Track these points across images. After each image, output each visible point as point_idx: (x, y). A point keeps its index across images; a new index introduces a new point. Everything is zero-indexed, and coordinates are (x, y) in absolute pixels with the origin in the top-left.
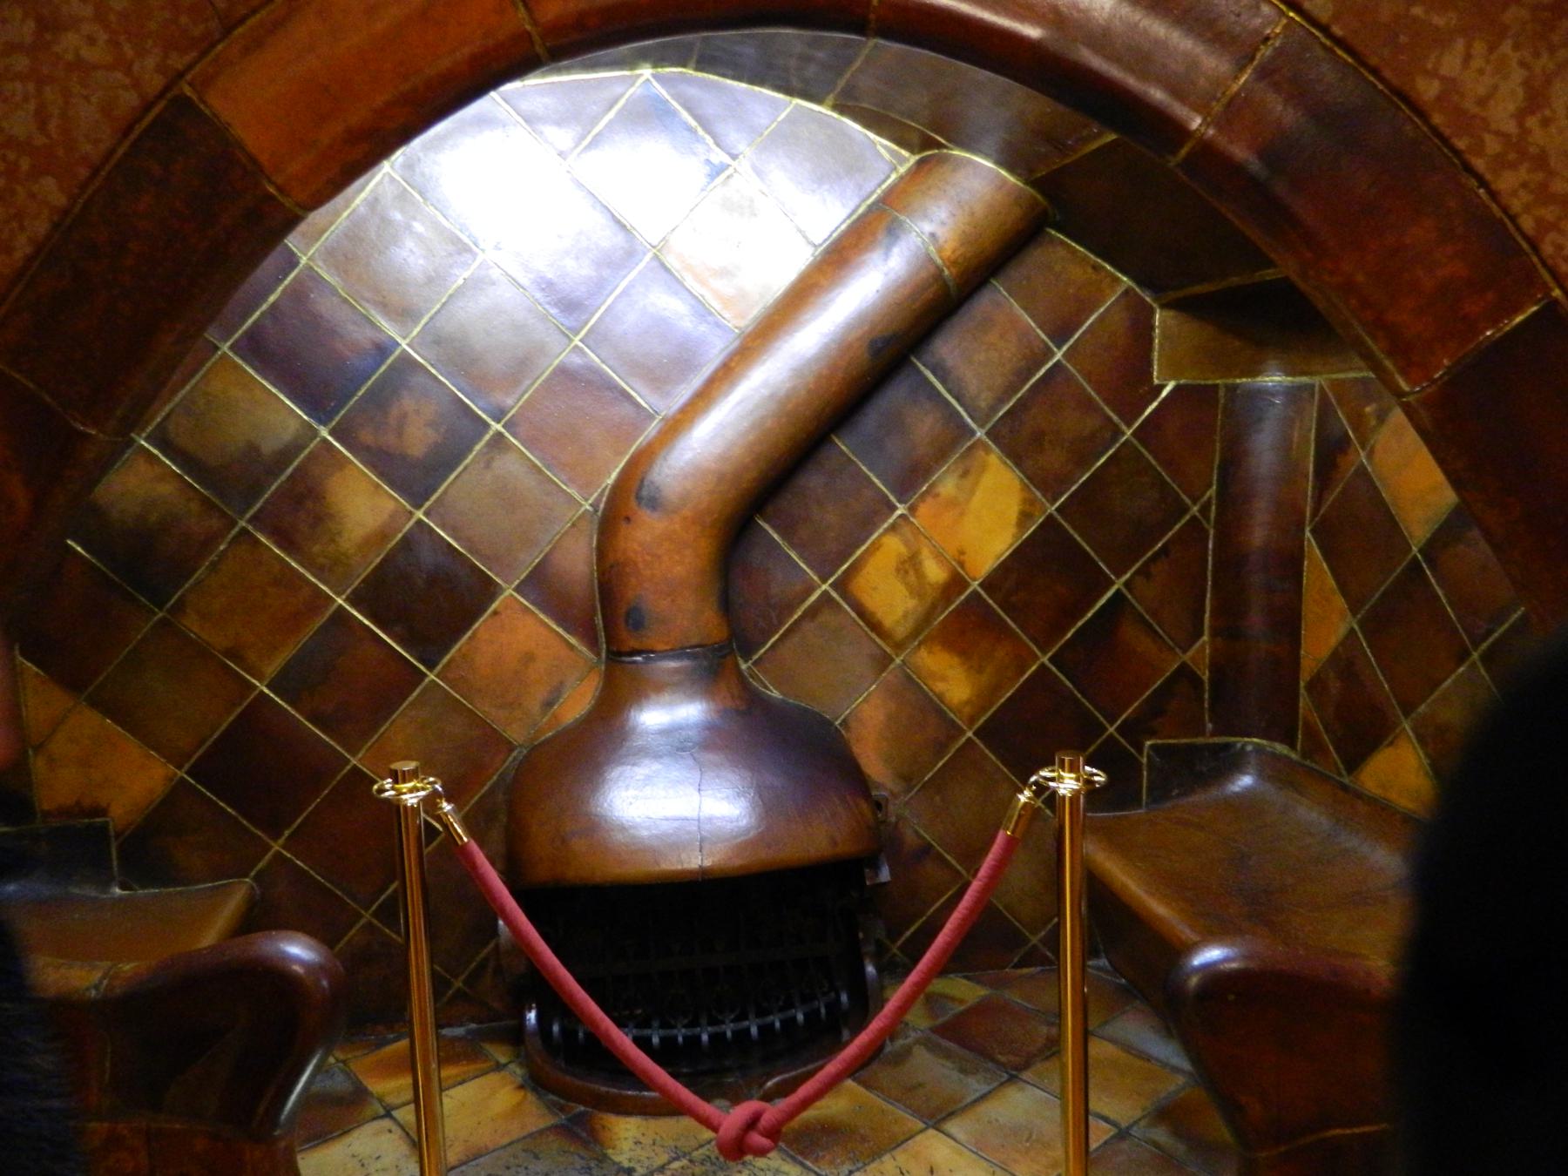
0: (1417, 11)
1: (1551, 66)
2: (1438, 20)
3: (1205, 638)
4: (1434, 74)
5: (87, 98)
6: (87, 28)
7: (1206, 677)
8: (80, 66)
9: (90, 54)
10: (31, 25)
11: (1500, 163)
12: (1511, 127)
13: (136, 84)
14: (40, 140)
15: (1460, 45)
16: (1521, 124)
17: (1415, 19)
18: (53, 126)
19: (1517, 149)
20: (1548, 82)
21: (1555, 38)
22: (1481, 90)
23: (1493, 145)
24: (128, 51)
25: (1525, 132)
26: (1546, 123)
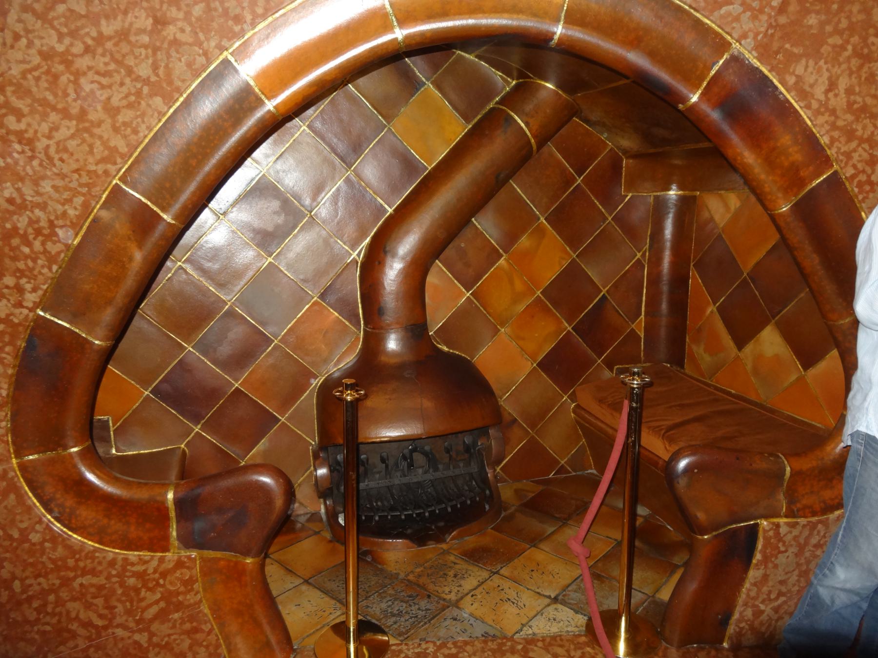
0: (787, 46)
1: (839, 72)
2: (796, 50)
3: (643, 316)
4: (793, 73)
5: (180, 61)
6: (180, 24)
7: (642, 336)
8: (175, 43)
10: (150, 21)
11: (817, 113)
13: (205, 54)
15: (804, 61)
16: (826, 96)
17: (787, 49)
18: (161, 72)
19: (825, 108)
20: (838, 78)
21: (841, 59)
22: (812, 81)
23: (815, 105)
24: (201, 36)
25: (828, 99)
26: (836, 95)
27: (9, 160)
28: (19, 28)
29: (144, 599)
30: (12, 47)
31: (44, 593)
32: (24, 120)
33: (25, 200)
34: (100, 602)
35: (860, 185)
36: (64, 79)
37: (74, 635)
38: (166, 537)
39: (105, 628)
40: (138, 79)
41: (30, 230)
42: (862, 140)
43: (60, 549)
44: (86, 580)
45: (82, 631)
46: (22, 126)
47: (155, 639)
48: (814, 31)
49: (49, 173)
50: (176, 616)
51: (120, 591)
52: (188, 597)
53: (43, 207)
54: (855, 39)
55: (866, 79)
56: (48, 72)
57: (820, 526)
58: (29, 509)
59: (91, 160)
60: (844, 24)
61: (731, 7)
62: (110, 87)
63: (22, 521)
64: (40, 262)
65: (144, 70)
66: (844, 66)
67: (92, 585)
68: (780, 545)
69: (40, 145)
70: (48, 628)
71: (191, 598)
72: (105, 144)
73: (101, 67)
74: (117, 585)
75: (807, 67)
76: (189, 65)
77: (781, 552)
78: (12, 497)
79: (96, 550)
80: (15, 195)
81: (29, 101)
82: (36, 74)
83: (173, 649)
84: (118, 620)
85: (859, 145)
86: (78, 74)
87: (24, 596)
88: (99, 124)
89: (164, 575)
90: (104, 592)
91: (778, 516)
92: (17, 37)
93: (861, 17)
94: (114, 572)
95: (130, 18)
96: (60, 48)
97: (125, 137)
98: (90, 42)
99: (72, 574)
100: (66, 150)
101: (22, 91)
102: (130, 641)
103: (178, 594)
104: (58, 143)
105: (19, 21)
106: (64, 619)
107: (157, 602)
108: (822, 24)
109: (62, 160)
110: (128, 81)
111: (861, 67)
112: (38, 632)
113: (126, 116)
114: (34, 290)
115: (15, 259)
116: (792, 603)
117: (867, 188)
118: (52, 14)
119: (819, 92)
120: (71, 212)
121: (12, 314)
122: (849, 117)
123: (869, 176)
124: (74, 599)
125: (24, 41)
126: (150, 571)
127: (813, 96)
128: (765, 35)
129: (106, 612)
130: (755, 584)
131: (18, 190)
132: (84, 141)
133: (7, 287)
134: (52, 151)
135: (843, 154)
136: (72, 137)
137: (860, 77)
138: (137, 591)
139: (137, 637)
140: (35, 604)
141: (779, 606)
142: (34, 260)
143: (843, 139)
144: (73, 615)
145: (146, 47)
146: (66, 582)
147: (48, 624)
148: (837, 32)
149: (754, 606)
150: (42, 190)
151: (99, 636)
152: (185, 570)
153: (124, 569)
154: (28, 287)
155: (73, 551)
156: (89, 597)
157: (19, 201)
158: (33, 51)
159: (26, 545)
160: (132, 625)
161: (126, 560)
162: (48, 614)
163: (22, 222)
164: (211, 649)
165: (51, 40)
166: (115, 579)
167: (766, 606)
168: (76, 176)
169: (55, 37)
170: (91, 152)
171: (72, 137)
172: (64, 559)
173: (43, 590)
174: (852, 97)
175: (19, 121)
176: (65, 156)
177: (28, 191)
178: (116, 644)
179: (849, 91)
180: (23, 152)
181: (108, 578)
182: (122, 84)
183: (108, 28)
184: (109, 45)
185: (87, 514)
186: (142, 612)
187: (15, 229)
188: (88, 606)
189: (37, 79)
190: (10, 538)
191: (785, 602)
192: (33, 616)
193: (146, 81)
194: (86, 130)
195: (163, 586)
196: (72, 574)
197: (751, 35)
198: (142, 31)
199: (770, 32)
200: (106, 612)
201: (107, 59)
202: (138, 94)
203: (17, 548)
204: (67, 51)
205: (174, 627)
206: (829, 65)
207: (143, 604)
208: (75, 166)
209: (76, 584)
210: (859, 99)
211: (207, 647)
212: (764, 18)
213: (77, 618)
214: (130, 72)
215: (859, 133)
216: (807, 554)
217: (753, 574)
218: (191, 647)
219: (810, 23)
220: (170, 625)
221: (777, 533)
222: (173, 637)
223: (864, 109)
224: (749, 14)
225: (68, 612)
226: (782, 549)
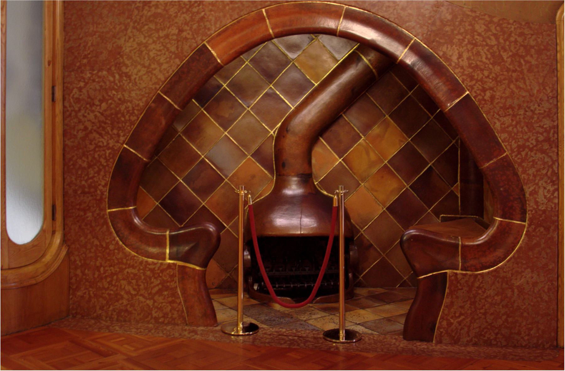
0: (437, 39)
4: (441, 50)
6: (188, 32)
8: (186, 39)
9: (188, 36)
10: (177, 31)
11: (455, 68)
12: (456, 61)
13: (196, 42)
14: (176, 52)
15: (446, 46)
18: (179, 49)
19: (458, 65)
20: (462, 53)
22: (450, 54)
23: (453, 64)
24: (195, 36)
25: (459, 62)
26: (463, 60)
27: (121, 84)
28: (131, 35)
29: (152, 283)
30: (128, 41)
31: (112, 275)
32: (129, 69)
33: (125, 99)
34: (134, 281)
35: (479, 101)
36: (144, 53)
37: (122, 298)
38: (165, 253)
39: (135, 295)
40: (171, 52)
41: (125, 111)
42: (477, 81)
43: (121, 254)
44: (130, 270)
45: (126, 296)
46: (128, 70)
47: (156, 304)
48: (449, 33)
49: (135, 88)
50: (166, 293)
51: (143, 278)
52: (172, 284)
53: (131, 102)
54: (468, 37)
55: (476, 54)
56: (139, 50)
57: (479, 276)
58: (111, 233)
59: (151, 83)
60: (462, 30)
61: (410, 23)
62: (160, 55)
63: (107, 239)
64: (127, 124)
65: (173, 49)
66: (465, 48)
67: (132, 273)
68: (459, 285)
69: (133, 78)
70: (112, 292)
71: (173, 285)
72: (156, 77)
73: (158, 48)
74: (142, 275)
75: (447, 48)
76: (190, 46)
77: (460, 289)
78: (105, 227)
79: (135, 256)
80: (122, 97)
81: (131, 61)
82: (135, 51)
83: (163, 310)
84: (142, 292)
85: (476, 83)
86: (150, 51)
87: (104, 275)
88: (155, 69)
89: (162, 271)
90: (137, 277)
91: (457, 269)
92: (130, 38)
93: (470, 28)
94: (141, 268)
95: (170, 30)
96: (144, 41)
97: (164, 74)
98: (155, 39)
99: (124, 267)
100: (142, 79)
101: (130, 58)
102: (145, 304)
103: (168, 282)
104: (139, 77)
105: (131, 32)
106: (119, 289)
107: (158, 285)
108: (452, 31)
109: (140, 83)
110: (167, 53)
111: (472, 49)
112: (108, 294)
113: (165, 66)
114: (124, 136)
115: (118, 123)
116: (468, 320)
117: (483, 102)
118: (143, 29)
119: (455, 58)
120: (141, 104)
121: (114, 146)
122: (471, 70)
123: (483, 97)
124: (124, 279)
125: (132, 39)
126: (156, 269)
127: (452, 60)
128: (427, 34)
129: (136, 287)
130: (447, 307)
131: (123, 95)
132: (149, 76)
133: (114, 134)
134: (137, 80)
135: (469, 86)
136: (145, 75)
137: (473, 53)
138: (150, 278)
139: (148, 302)
140: (109, 280)
141: (461, 321)
142: (125, 123)
143: (468, 80)
144: (123, 287)
145: (175, 40)
146: (122, 270)
147: (112, 290)
148: (459, 33)
149: (447, 319)
150: (131, 95)
151: (132, 298)
152: (171, 270)
153: (146, 267)
154: (122, 134)
155: (127, 255)
156: (130, 279)
157: (123, 99)
158: (135, 43)
159: (108, 251)
160: (147, 295)
161: (147, 262)
162: (112, 285)
163: (123, 108)
164: (180, 312)
165: (142, 39)
166: (142, 271)
167: (454, 320)
168: (144, 90)
169: (142, 36)
170: (151, 80)
171: (145, 75)
172: (122, 259)
173: (112, 273)
174: (470, 61)
175: (127, 69)
176: (141, 82)
177: (126, 95)
178: (139, 304)
179: (469, 59)
180: (126, 80)
181: (139, 270)
182: (165, 54)
183: (162, 34)
184: (162, 40)
185: (132, 239)
186: (152, 289)
187: (120, 110)
188: (130, 283)
189: (135, 53)
190: (102, 246)
191: (464, 319)
192: (106, 286)
193: (174, 53)
194: (150, 72)
195: (161, 277)
196: (124, 267)
197: (420, 34)
198: (174, 34)
199: (429, 33)
200: (136, 287)
201: (160, 45)
202: (170, 58)
203: (104, 252)
204: (147, 43)
205: (164, 299)
206: (458, 47)
207: (152, 285)
208: (144, 86)
209: (125, 272)
210: (474, 62)
211: (178, 311)
212: (426, 28)
213: (124, 288)
214: (168, 49)
215: (476, 77)
216: (474, 292)
217: (446, 301)
218: (171, 311)
219: (447, 29)
220: (163, 297)
221: (456, 278)
222: (164, 304)
223: (477, 66)
224: (418, 26)
225: (121, 286)
226: (460, 287)
